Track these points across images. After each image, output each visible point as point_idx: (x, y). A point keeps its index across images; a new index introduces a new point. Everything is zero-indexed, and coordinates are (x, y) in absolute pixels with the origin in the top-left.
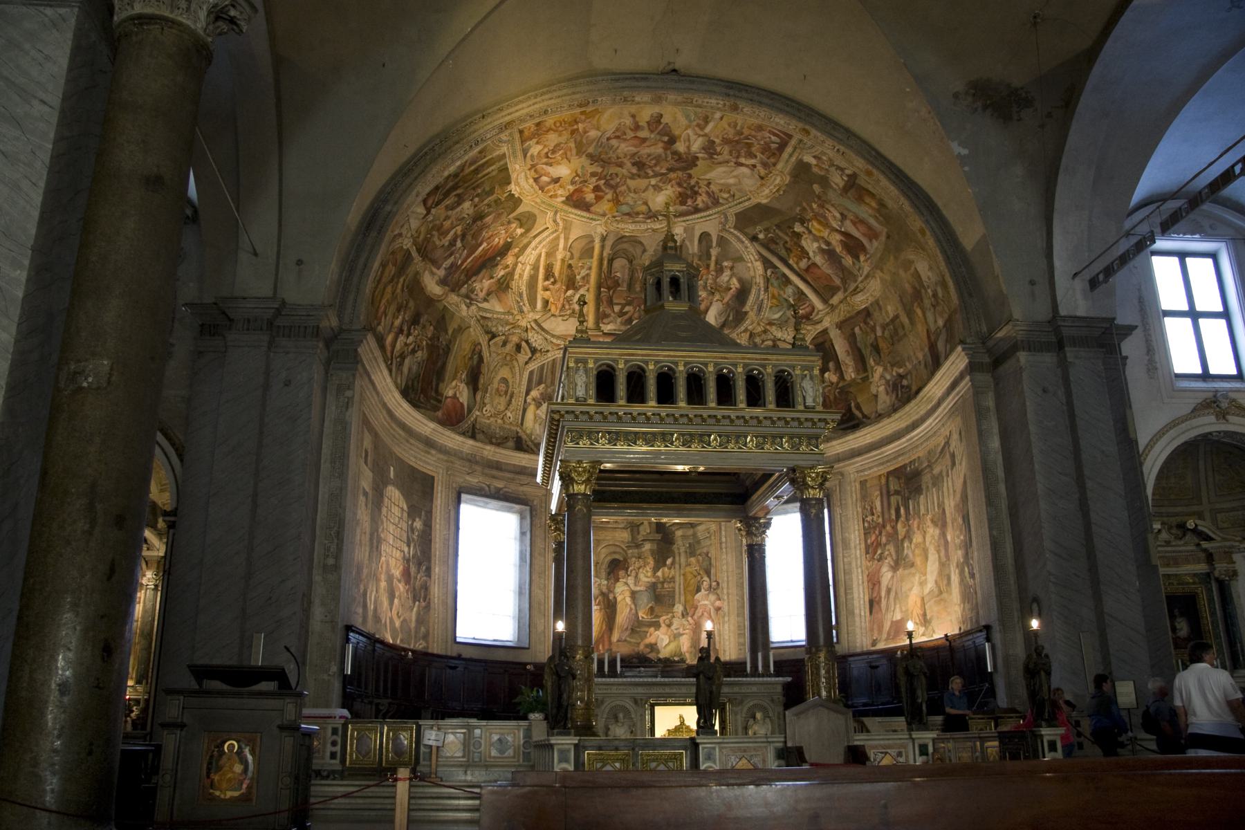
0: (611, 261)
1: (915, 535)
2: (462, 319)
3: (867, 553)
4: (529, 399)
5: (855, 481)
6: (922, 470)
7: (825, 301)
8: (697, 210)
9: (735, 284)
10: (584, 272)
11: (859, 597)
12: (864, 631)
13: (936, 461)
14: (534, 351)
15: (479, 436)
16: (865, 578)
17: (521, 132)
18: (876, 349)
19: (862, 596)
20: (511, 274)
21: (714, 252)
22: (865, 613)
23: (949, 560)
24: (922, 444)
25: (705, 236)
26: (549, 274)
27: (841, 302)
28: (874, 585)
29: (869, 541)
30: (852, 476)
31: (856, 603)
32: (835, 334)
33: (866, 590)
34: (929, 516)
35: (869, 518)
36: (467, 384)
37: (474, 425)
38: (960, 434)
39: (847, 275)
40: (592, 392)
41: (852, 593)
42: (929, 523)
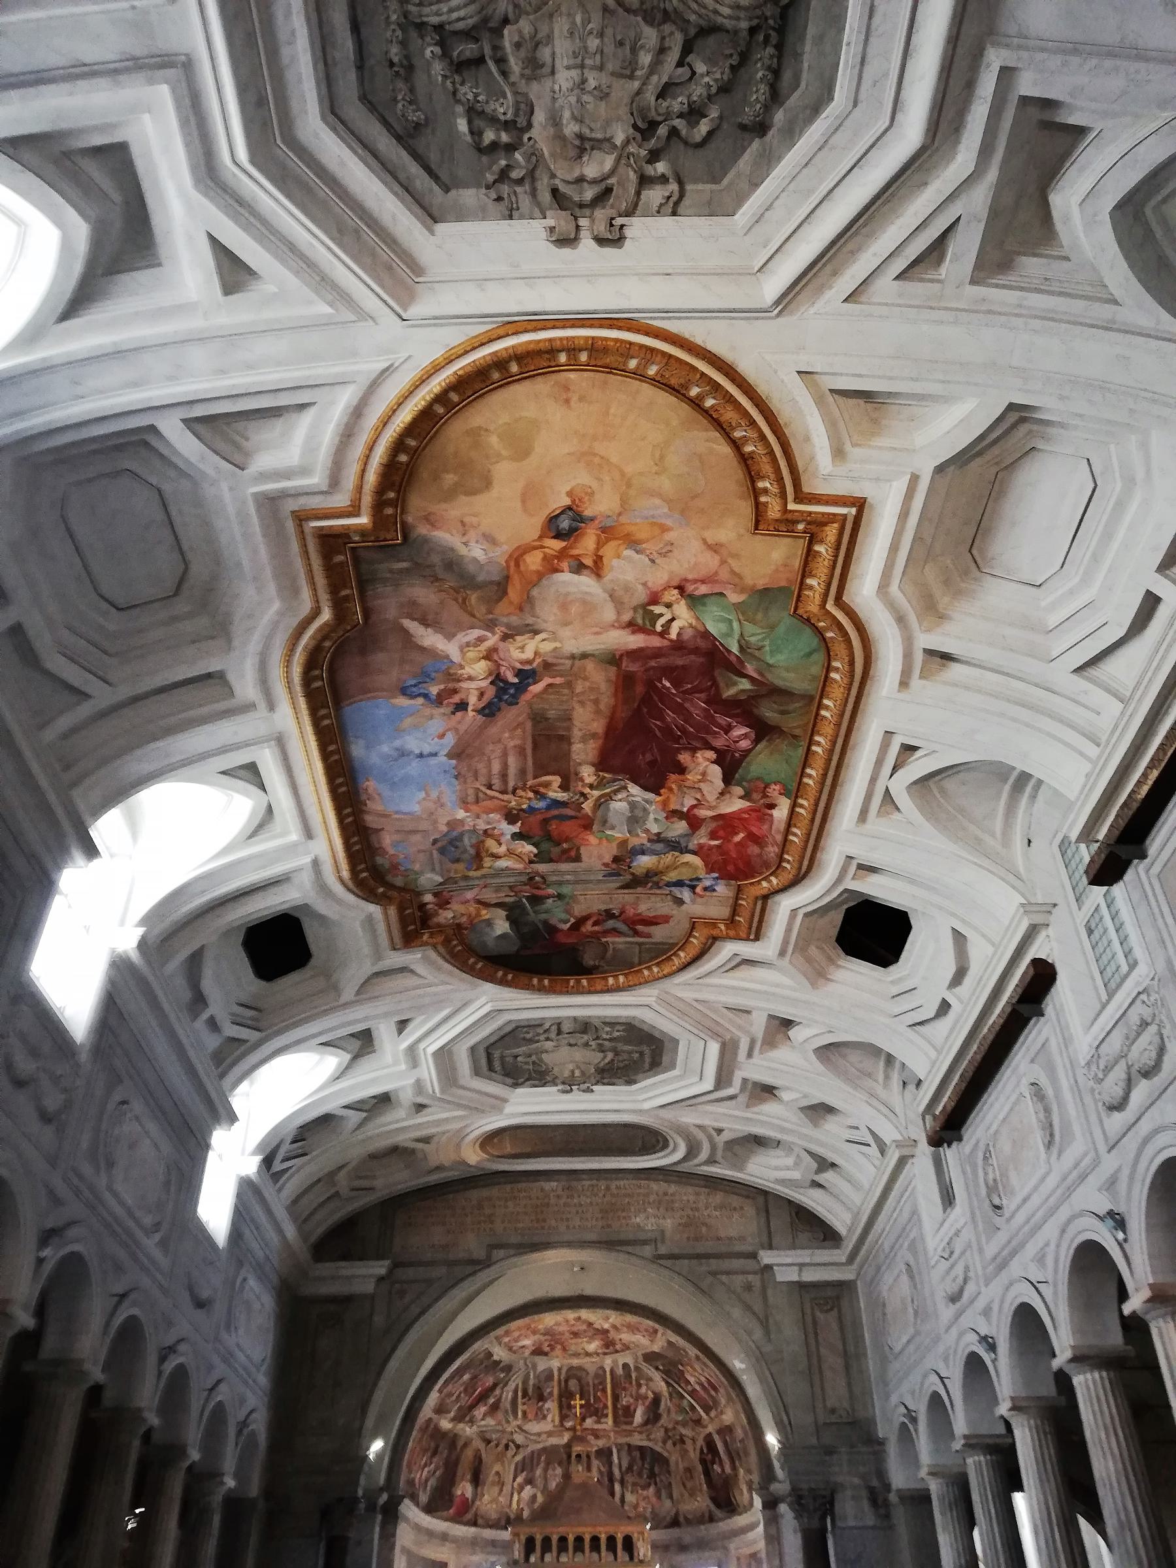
0: (566, 1381)
2: (467, 1437)
4: (515, 1485)
7: (707, 1414)
8: (617, 1352)
9: (651, 1395)
10: (548, 1390)
14: (518, 1447)
15: (480, 1521)
17: (496, 1338)
18: (738, 1454)
20: (499, 1401)
21: (634, 1375)
25: (625, 1366)
26: (525, 1394)
27: (716, 1416)
32: (716, 1437)
36: (471, 1482)
37: (476, 1515)
39: (716, 1403)
40: (522, 1555)
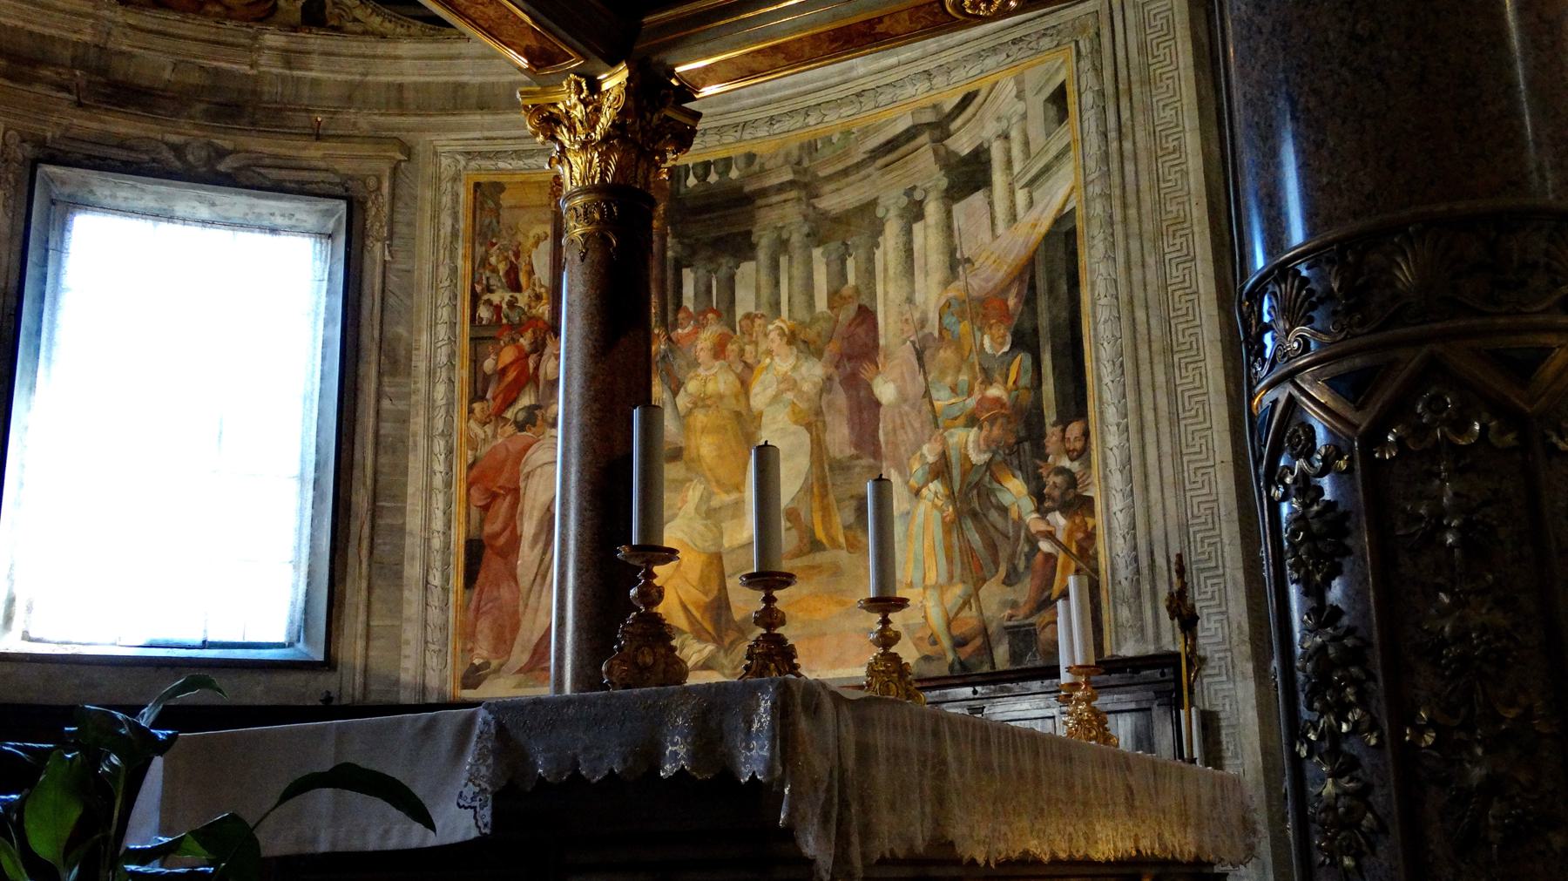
1: (701, 371)
3: (477, 395)
5: (455, 179)
6: (763, 193)
11: (427, 526)
12: (434, 635)
13: (845, 172)
16: (460, 470)
19: (438, 524)
22: (446, 579)
23: (876, 453)
24: (772, 120)
28: (494, 496)
29: (488, 365)
30: (445, 162)
31: (413, 545)
33: (458, 509)
34: (783, 322)
35: (500, 297)
38: (1059, 98)
41: (402, 511)
42: (775, 341)
